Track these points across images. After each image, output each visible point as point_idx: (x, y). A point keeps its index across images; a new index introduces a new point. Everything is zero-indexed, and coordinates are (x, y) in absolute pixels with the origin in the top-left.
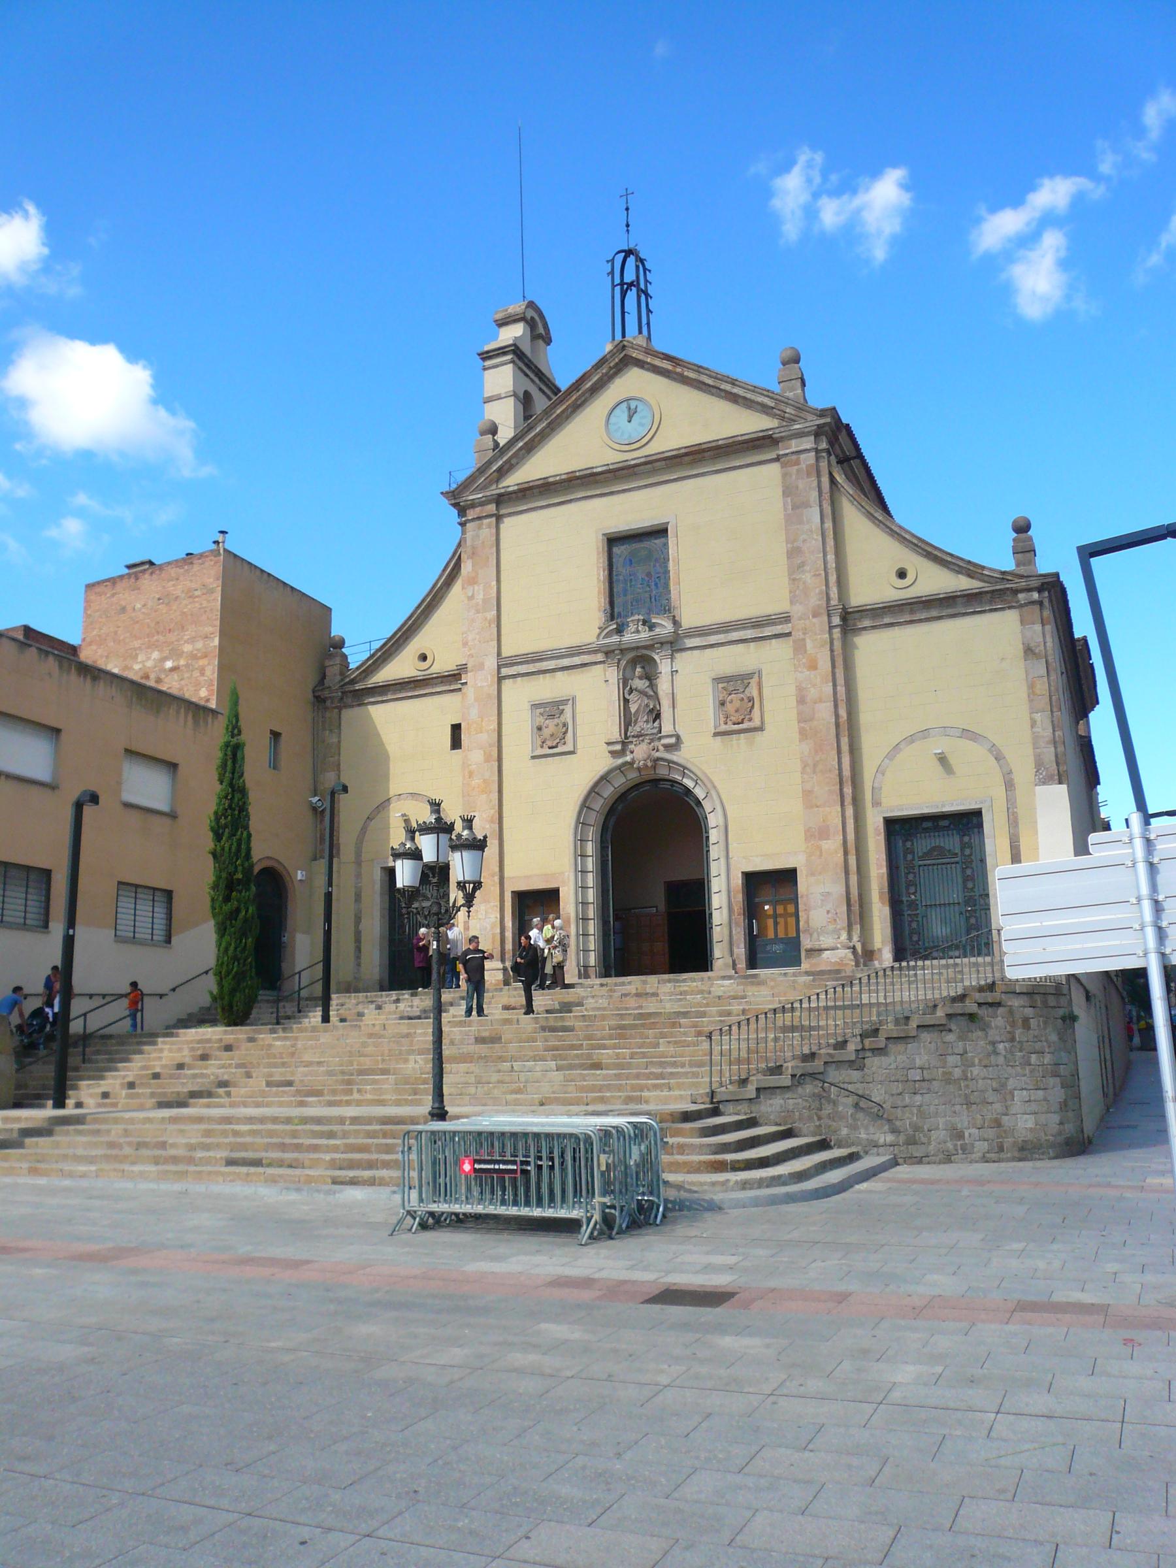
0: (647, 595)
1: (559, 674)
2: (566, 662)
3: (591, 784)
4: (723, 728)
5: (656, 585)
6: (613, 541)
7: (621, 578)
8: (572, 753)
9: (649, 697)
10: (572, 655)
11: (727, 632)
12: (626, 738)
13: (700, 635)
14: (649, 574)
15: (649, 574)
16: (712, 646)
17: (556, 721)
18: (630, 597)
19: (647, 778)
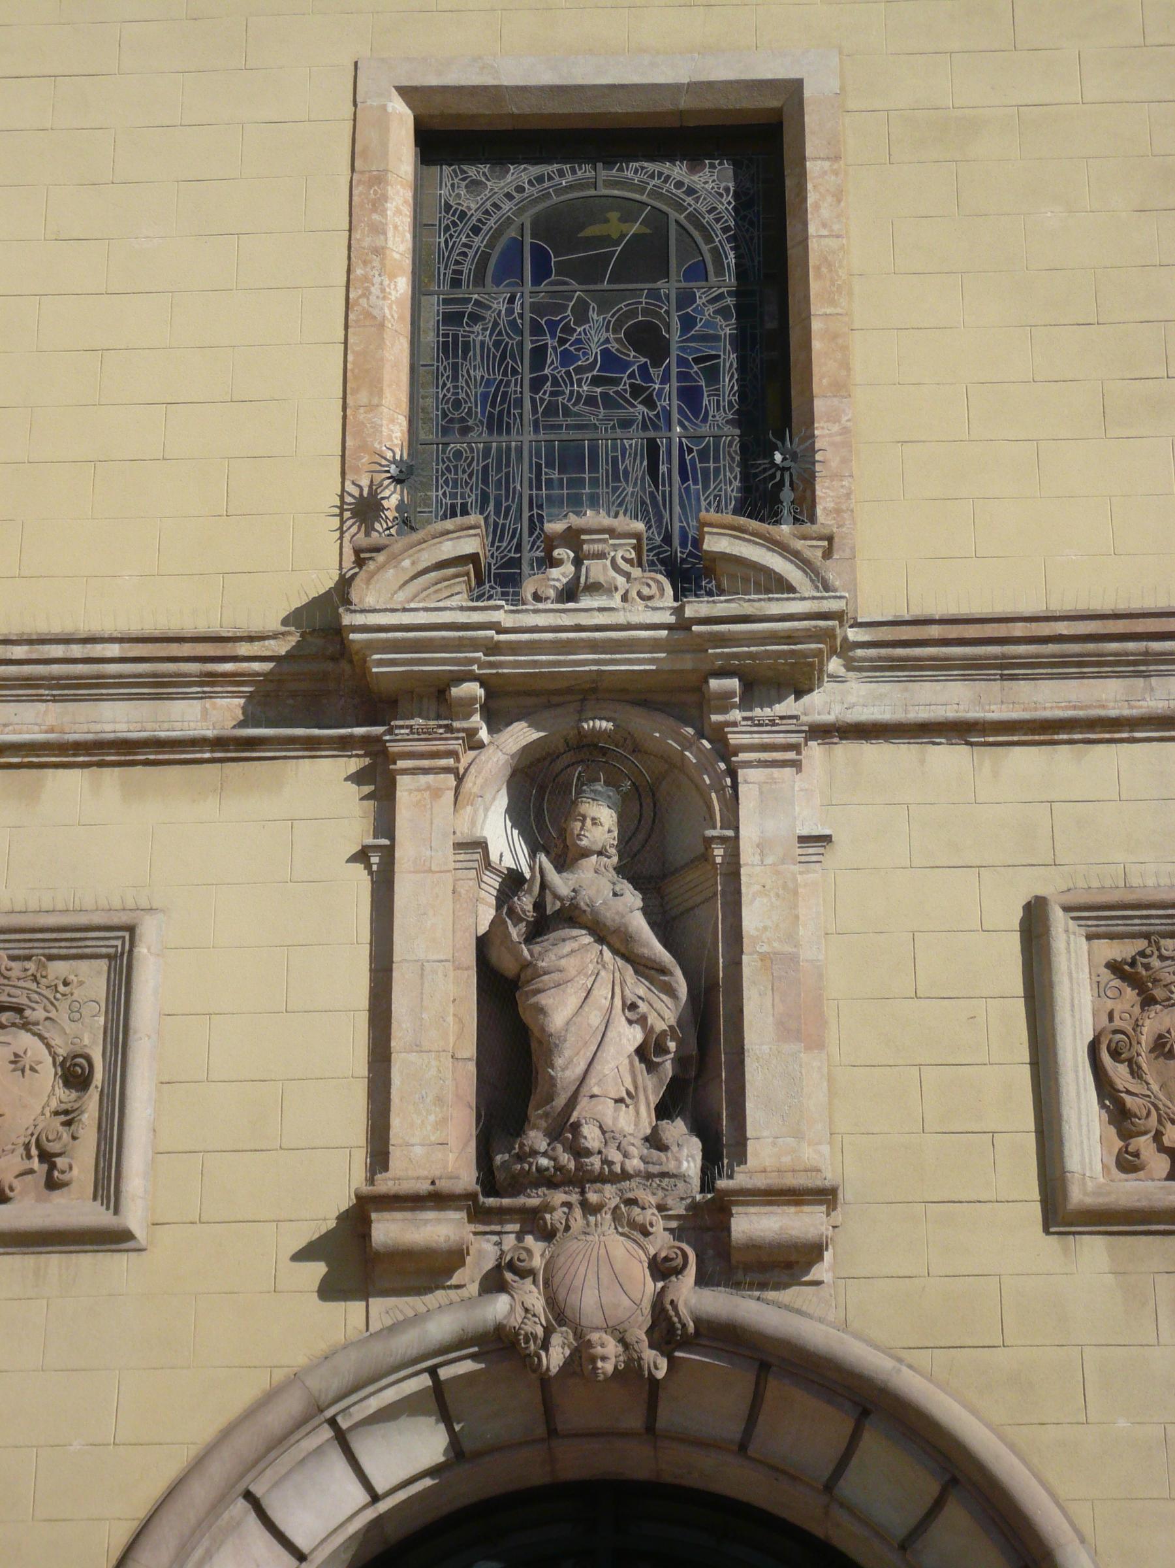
0: (634, 440)
1: (68, 785)
2: (117, 718)
3: (246, 1443)
4: (1131, 1191)
5: (690, 397)
6: (454, 135)
7: (479, 335)
8: (114, 1239)
9: (645, 968)
10: (161, 687)
11: (1138, 667)
12: (489, 1180)
13: (972, 669)
14: (648, 339)
15: (648, 339)
16: (1044, 731)
17: (25, 1041)
18: (525, 437)
19: (577, 1462)
